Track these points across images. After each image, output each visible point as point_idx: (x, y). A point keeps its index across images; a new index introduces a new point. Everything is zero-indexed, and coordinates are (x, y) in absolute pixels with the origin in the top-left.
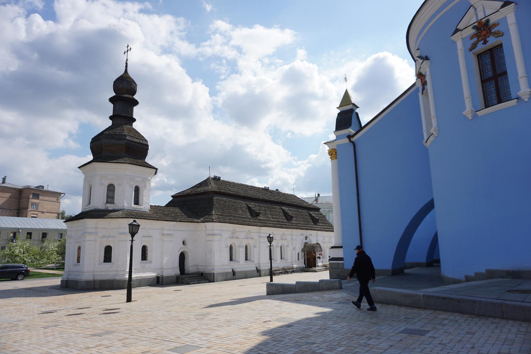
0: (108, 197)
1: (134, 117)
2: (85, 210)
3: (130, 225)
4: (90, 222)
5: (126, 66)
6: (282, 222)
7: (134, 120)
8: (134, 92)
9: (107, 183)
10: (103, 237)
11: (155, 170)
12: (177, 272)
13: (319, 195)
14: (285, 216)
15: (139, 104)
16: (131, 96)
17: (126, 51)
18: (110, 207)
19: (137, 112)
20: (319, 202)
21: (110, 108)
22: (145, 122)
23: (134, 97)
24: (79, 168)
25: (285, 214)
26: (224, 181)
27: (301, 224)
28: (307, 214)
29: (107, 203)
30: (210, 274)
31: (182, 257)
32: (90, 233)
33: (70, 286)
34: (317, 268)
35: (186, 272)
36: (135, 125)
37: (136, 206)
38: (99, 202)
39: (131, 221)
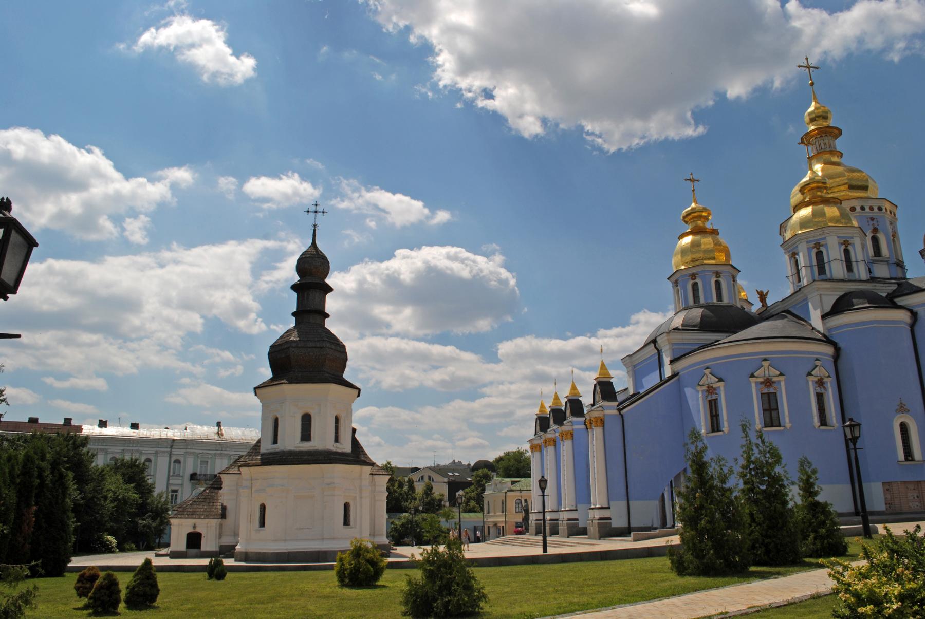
1: (327, 311)
7: (327, 316)
17: (313, 208)
23: (327, 281)
24: (255, 389)
38: (291, 440)
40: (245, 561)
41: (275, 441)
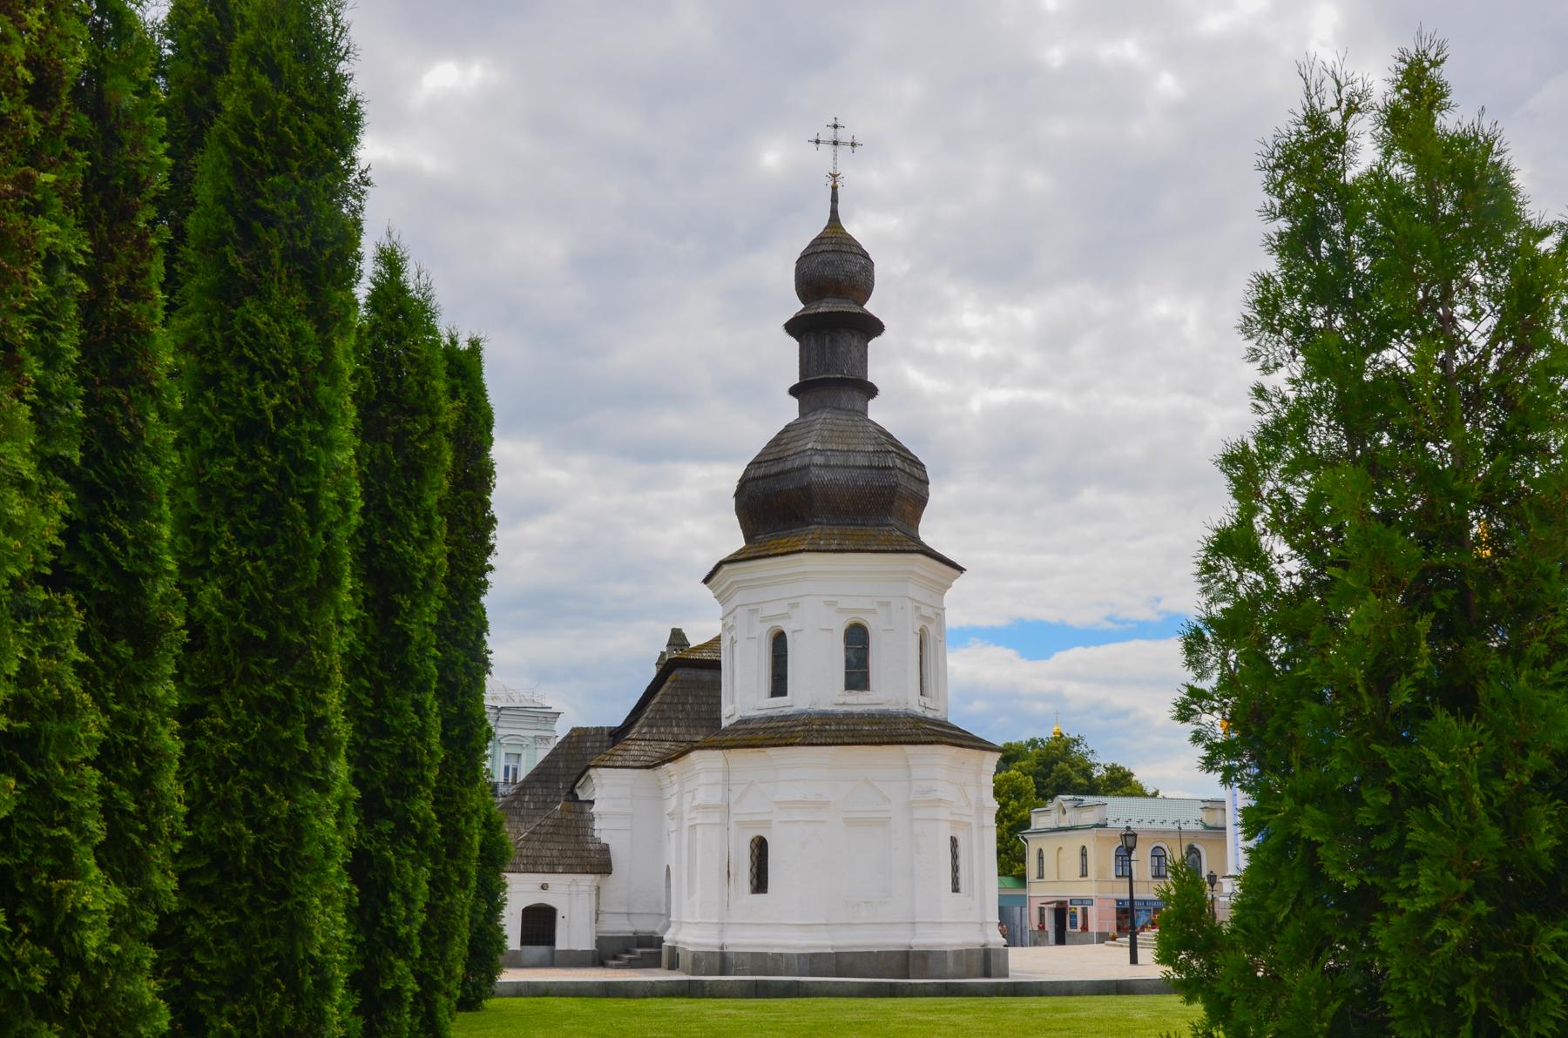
7: (871, 391)
8: (866, 292)
9: (840, 626)
15: (884, 335)
18: (859, 702)
21: (786, 357)
36: (876, 412)
38: (817, 685)
40: (752, 974)
41: (779, 686)
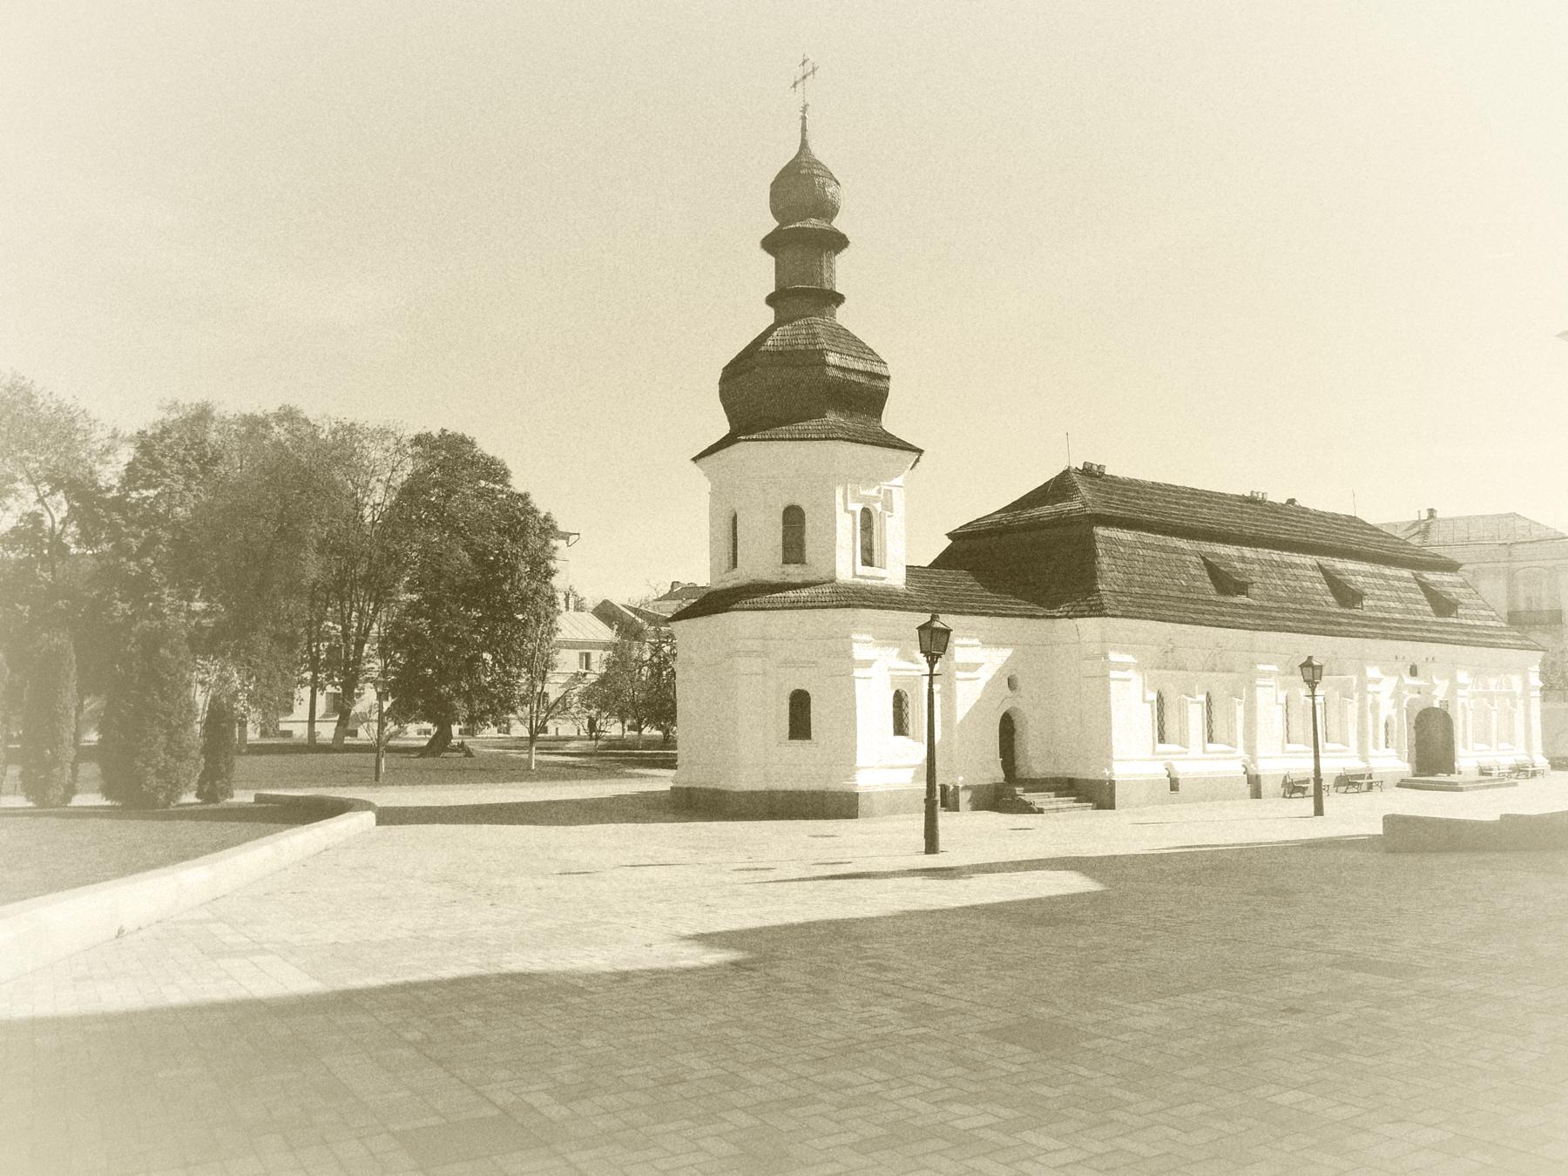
0: (787, 547)
1: (838, 289)
2: (721, 586)
3: (921, 628)
4: (741, 623)
5: (804, 129)
6: (1329, 614)
7: (839, 299)
10: (786, 663)
11: (915, 456)
12: (996, 774)
13: (1431, 511)
14: (1334, 592)
16: (824, 225)
17: (799, 77)
18: (795, 573)
19: (844, 272)
20: (1435, 537)
21: (763, 273)
22: (873, 303)
24: (695, 459)
25: (1336, 584)
26: (1114, 479)
27: (1395, 620)
28: (1415, 586)
29: (785, 562)
30: (1101, 783)
31: (1008, 728)
32: (749, 654)
33: (694, 804)
34: (1454, 778)
35: (1022, 771)
36: (843, 316)
37: (867, 570)
38: (761, 558)
39: (926, 617)
